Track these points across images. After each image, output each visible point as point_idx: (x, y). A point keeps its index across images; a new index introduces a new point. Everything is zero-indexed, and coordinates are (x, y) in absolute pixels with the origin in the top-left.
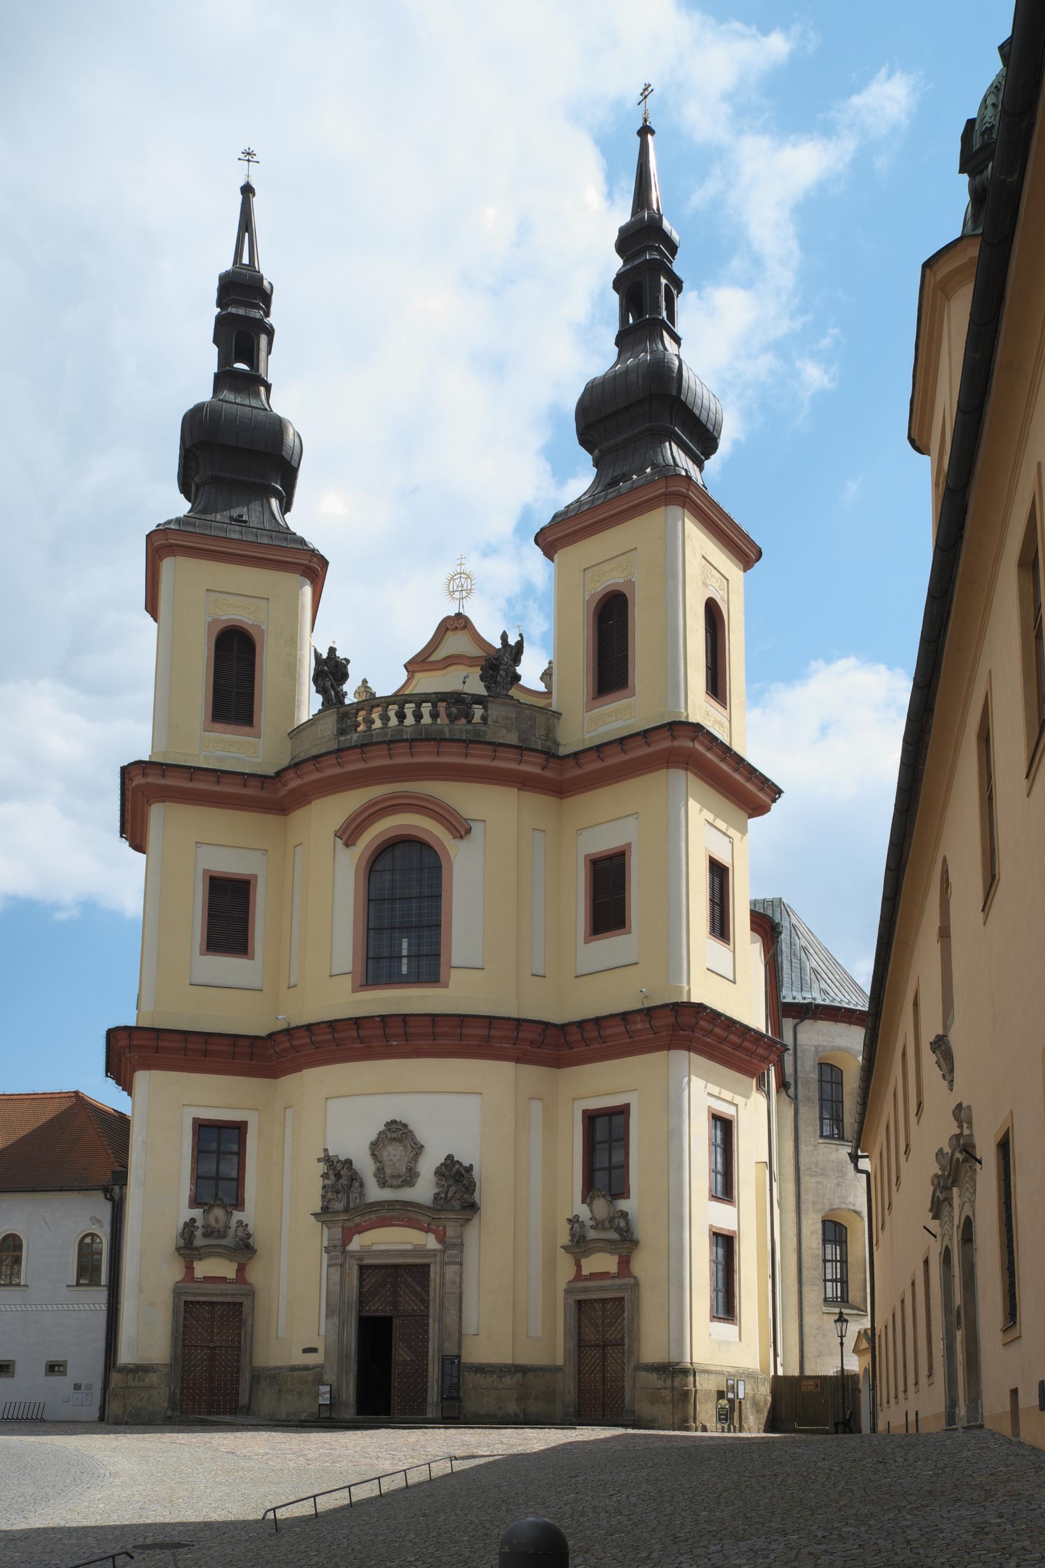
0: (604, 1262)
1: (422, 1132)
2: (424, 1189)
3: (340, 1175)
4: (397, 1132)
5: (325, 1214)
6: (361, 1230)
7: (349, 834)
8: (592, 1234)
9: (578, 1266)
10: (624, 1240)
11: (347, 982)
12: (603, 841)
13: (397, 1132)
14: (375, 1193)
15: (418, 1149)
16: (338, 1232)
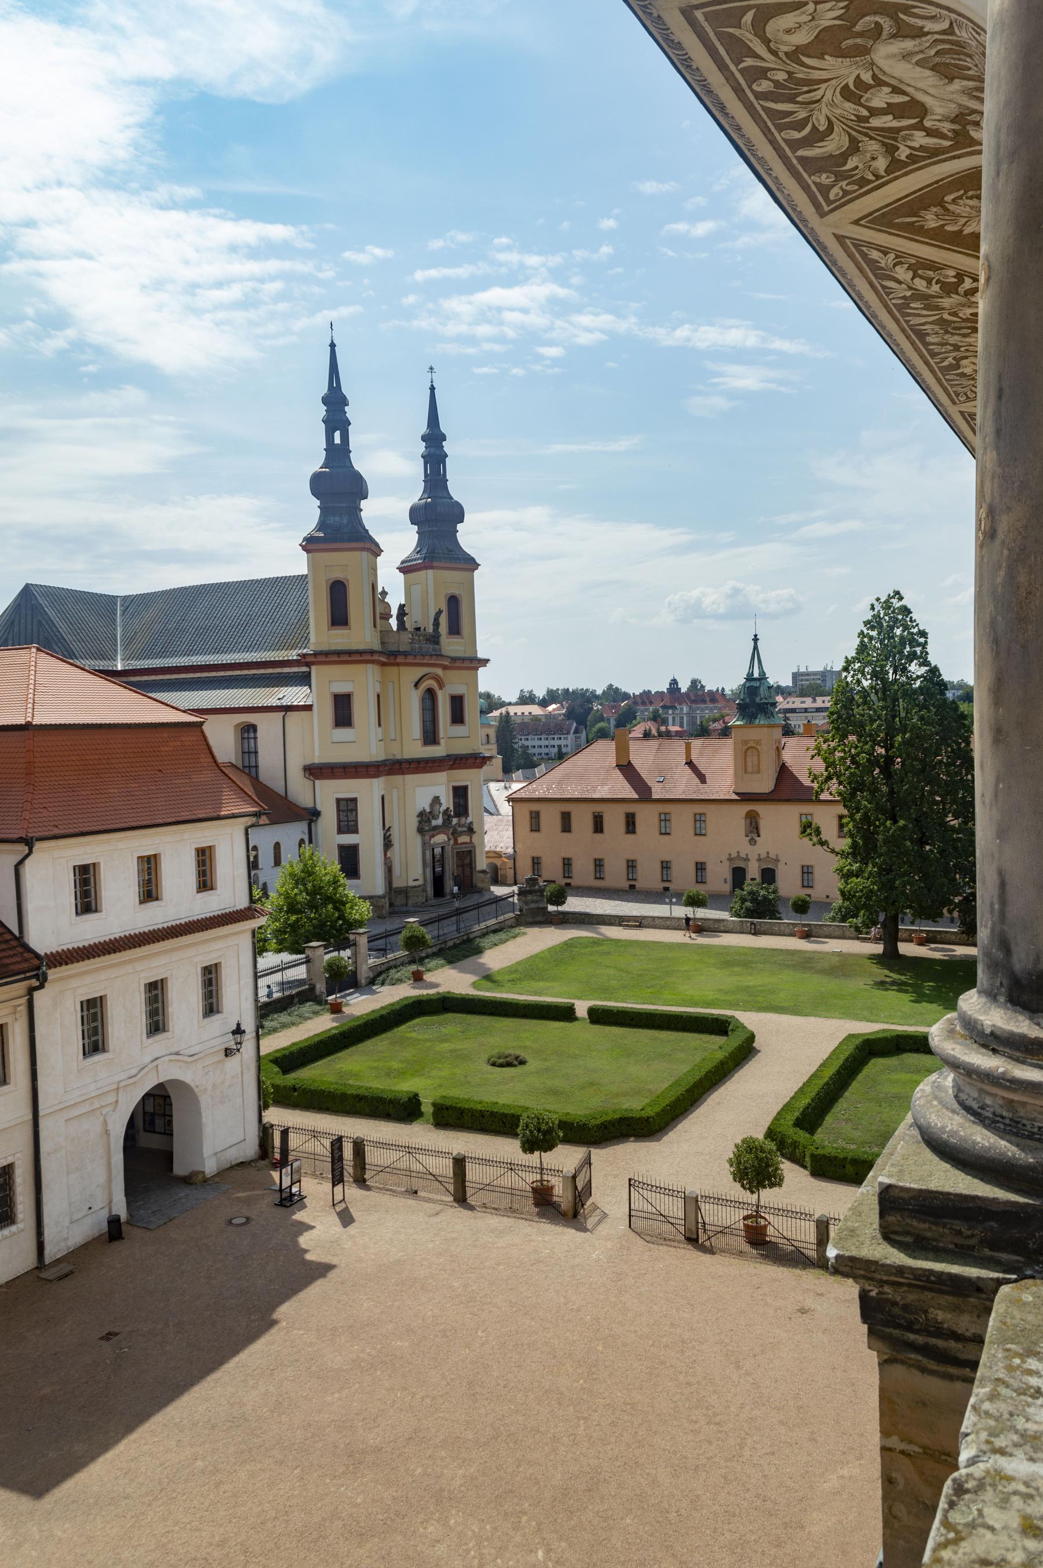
0: (464, 839)
1: (443, 800)
2: (439, 821)
3: (421, 814)
4: (436, 800)
5: (420, 831)
6: (433, 836)
7: (416, 685)
8: (460, 829)
9: (456, 840)
10: (471, 830)
11: (420, 743)
12: (458, 690)
13: (436, 800)
14: (434, 823)
15: (440, 804)
16: (427, 837)
